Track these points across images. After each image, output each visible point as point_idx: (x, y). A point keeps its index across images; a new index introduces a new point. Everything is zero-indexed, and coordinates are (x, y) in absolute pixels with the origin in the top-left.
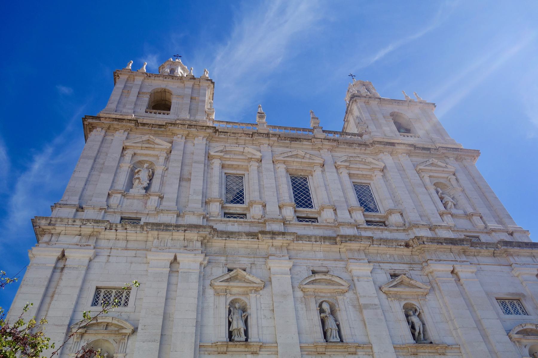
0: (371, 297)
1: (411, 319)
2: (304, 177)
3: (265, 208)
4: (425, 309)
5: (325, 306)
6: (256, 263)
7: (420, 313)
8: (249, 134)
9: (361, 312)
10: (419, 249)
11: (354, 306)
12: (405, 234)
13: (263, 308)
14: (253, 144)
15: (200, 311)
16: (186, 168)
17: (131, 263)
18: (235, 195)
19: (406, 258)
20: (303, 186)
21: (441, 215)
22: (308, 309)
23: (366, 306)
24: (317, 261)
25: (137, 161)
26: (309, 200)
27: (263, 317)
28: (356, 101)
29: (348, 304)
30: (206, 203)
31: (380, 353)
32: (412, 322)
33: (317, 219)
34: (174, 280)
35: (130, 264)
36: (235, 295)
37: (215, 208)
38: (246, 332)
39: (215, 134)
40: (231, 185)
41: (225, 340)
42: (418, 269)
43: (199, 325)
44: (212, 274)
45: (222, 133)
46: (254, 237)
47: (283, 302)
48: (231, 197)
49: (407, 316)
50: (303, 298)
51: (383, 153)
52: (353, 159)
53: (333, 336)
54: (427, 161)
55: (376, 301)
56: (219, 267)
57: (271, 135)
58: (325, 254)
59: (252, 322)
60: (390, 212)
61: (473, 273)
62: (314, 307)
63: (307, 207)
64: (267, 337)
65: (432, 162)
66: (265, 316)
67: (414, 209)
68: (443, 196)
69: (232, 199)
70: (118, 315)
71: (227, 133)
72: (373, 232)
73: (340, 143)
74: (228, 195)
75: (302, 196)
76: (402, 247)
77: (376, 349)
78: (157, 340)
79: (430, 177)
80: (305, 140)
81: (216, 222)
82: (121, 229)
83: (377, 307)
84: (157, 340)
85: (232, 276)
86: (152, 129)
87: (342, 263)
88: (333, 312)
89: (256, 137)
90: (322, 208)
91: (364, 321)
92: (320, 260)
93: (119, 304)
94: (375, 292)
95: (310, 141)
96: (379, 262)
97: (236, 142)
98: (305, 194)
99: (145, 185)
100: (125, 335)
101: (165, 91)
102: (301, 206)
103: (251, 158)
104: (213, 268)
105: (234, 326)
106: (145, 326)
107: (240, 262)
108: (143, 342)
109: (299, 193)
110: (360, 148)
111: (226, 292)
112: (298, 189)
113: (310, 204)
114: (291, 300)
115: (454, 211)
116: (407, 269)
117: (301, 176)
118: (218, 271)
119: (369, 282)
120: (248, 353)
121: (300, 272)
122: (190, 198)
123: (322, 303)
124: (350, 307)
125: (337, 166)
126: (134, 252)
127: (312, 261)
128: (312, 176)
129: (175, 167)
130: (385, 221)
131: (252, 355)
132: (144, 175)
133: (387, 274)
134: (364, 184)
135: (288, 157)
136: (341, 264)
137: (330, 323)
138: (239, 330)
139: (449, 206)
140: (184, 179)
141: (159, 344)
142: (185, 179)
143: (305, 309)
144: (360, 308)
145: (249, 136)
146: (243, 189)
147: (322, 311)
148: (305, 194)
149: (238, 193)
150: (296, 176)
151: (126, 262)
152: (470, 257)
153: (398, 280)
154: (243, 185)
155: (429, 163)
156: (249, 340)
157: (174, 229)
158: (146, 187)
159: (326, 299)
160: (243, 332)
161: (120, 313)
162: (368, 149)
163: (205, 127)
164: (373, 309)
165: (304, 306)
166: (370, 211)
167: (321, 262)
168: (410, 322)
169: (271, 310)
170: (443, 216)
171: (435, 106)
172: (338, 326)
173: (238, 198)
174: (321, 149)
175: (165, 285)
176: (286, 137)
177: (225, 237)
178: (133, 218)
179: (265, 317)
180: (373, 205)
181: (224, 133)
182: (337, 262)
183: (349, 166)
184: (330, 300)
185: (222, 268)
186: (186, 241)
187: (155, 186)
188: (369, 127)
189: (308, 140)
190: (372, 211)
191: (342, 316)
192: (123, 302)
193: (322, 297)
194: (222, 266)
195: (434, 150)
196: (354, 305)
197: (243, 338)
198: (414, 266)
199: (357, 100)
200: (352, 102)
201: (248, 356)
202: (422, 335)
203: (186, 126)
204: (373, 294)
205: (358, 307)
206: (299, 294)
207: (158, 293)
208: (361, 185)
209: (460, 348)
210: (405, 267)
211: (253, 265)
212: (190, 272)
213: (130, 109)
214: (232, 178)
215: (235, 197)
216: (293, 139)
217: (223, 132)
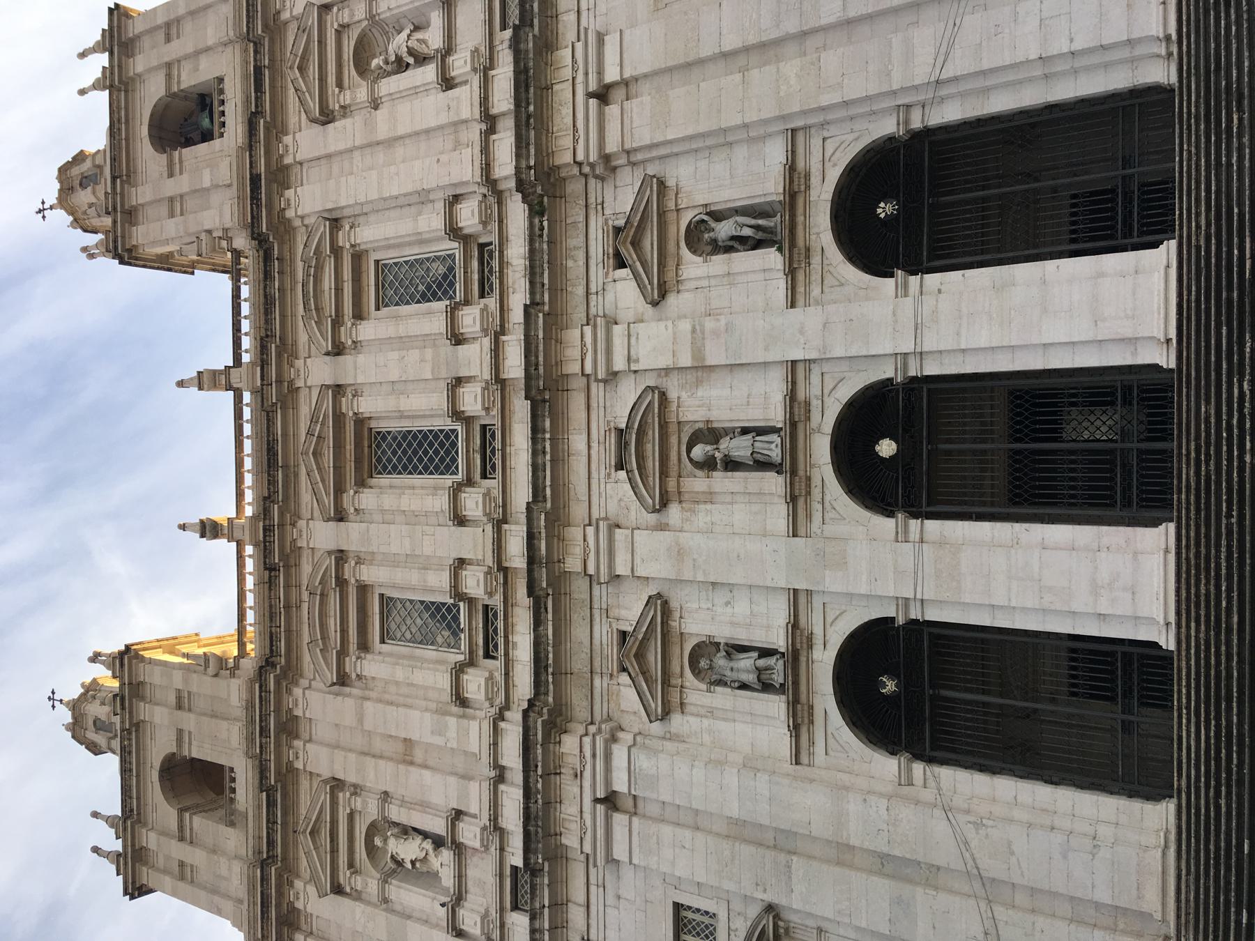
0: (674, 338)
1: (723, 241)
2: (376, 438)
3: (467, 561)
4: (701, 199)
5: (699, 451)
6: (604, 606)
7: (707, 214)
8: (270, 577)
9: (712, 368)
10: (549, 179)
11: (698, 383)
12: (508, 200)
13: (710, 605)
14: (296, 565)
16: (378, 745)
17: (619, 897)
18: (438, 625)
19: (573, 216)
20: (400, 445)
21: (447, 83)
22: (710, 497)
23: (698, 352)
24: (594, 452)
25: (366, 858)
26: (436, 436)
27: (729, 610)
28: (129, 251)
29: (694, 396)
31: (806, 346)
32: (733, 238)
33: (484, 427)
35: (621, 900)
36: (682, 667)
38: (765, 653)
39: (278, 666)
40: (412, 630)
41: (783, 706)
42: (599, 192)
44: (635, 713)
45: (274, 648)
46: (542, 605)
47: (694, 560)
48: (443, 633)
49: (718, 248)
50: (684, 505)
51: (284, 209)
52: (312, 299)
53: (773, 448)
54: (295, 88)
55: (685, 326)
56: (617, 695)
57: (267, 522)
58: (574, 429)
59: (743, 636)
60: (453, 231)
61: (603, 40)
63: (454, 444)
65: (297, 71)
66: (727, 603)
67: (438, 160)
68: (393, 58)
69: (446, 633)
70: (735, 935)
71: (271, 634)
72: (511, 290)
73: (269, 333)
74: (440, 640)
75: (426, 452)
76: (545, 224)
77: (797, 355)
78: (788, 862)
79: (340, 84)
80: (271, 429)
81: (511, 687)
82: (542, 920)
83: (698, 327)
84: (788, 862)
85: (638, 670)
86: (279, 822)
87: (594, 386)
89: (277, 561)
90: (456, 414)
91: (732, 367)
92: (589, 447)
93: (711, 928)
94: (662, 325)
95: (271, 414)
96: (588, 293)
97: (294, 609)
98: (420, 445)
99: (428, 845)
100: (776, 927)
101: (169, 769)
102: (454, 460)
103: (337, 578)
104: (622, 707)
105: (750, 678)
106: (757, 885)
107: (604, 641)
108: (792, 891)
109: (420, 460)
110: (276, 275)
112: (410, 460)
113: (447, 436)
114: (684, 538)
115: (434, 38)
116: (601, 220)
117: (374, 446)
119: (638, 334)
120: (810, 656)
121: (620, 500)
122: (455, 746)
123: (691, 460)
124: (700, 393)
125: (335, 350)
126: (593, 889)
127: (594, 466)
128: (370, 418)
130: (478, 244)
131: (814, 647)
133: (616, 277)
134: (380, 279)
135: (323, 481)
137: (740, 448)
138: (759, 671)
139: (423, 49)
140: (408, 753)
141: (795, 858)
142: (406, 750)
143: (709, 506)
144: (702, 370)
145: (276, 576)
146: (422, 602)
147: (708, 465)
148: (420, 445)
149: (433, 616)
150: (374, 460)
151: (618, 909)
152: (560, 32)
153: (628, 253)
154: (411, 601)
155: (300, 79)
156: (782, 650)
157: (536, 802)
158: (433, 845)
159: (684, 448)
160: (762, 663)
161: (731, 932)
162: (276, 252)
163: (263, 694)
164: (703, 339)
165: (702, 507)
166: (454, 276)
167: (594, 445)
168: (731, 243)
169: (713, 589)
170: (453, 78)
171: (117, 5)
172: (745, 431)
173: (444, 618)
174: (291, 382)
175: (667, 831)
176: (269, 480)
177: (547, 675)
178: (514, 883)
179: (730, 603)
180: (435, 265)
181: (274, 643)
182: (594, 404)
183: (334, 317)
184: (685, 440)
185: (622, 688)
186: (563, 771)
188: (206, 227)
189: (268, 420)
190: (451, 269)
191: (723, 416)
192: (706, 920)
193: (679, 460)
194: (615, 687)
195: (258, 56)
196: (695, 380)
198: (592, 200)
199: (127, 247)
200: (136, 260)
201: (815, 657)
202: (760, 222)
203: (264, 740)
204: (667, 329)
205: (700, 374)
206: (674, 511)
207: (684, 847)
208: (383, 286)
209: (792, 130)
211: (611, 614)
212: (635, 770)
213: (230, 869)
214: (393, 626)
215: (442, 625)
216: (272, 461)
217: (271, 645)
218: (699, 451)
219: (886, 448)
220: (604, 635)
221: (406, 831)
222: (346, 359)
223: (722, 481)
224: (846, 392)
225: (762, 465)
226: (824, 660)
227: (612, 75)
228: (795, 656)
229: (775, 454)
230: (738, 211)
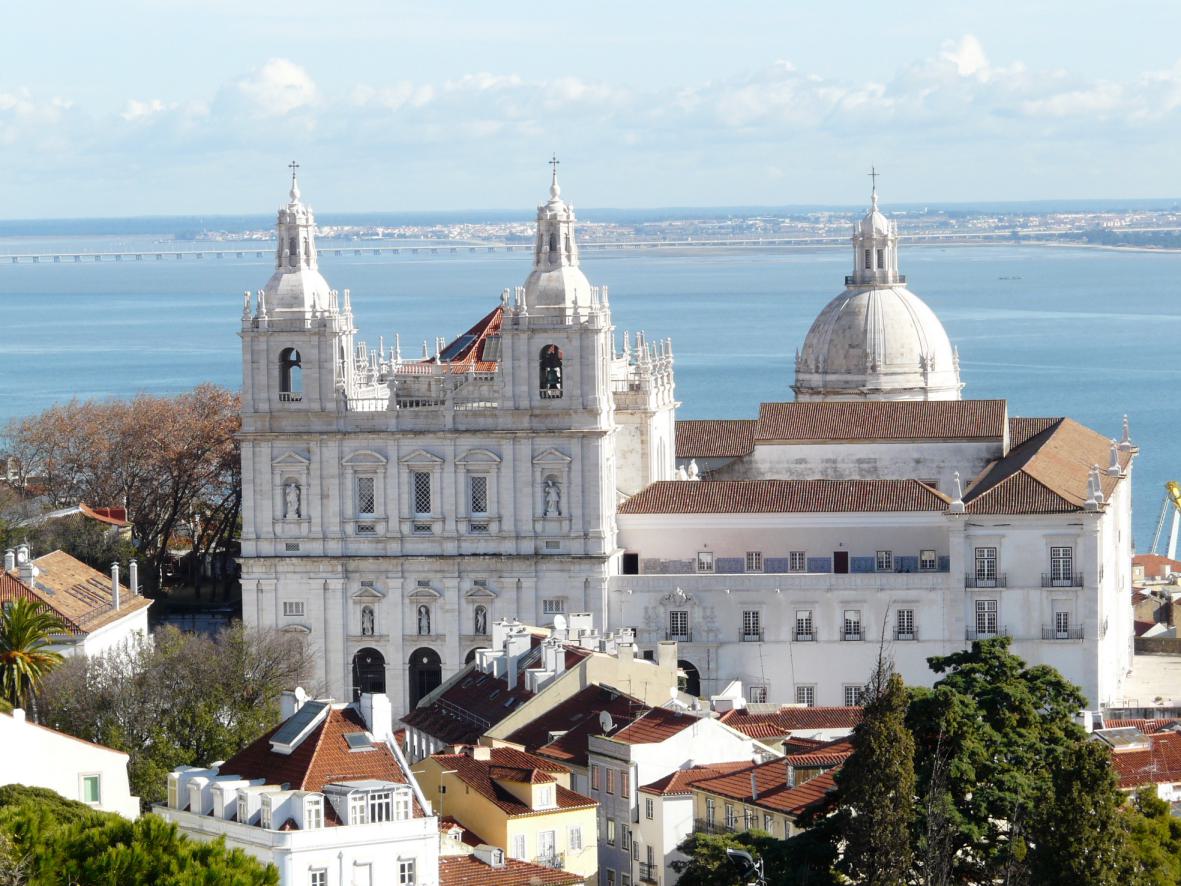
5: (423, 610)
15: (345, 616)
30: (343, 522)
34: (327, 595)
37: (350, 528)
38: (372, 629)
43: (345, 626)
49: (477, 614)
64: (384, 632)
88: (427, 612)
111: (360, 602)
118: (355, 587)
129: (316, 490)
137: (424, 623)
147: (420, 612)
187: (304, 512)
191: (432, 616)
197: (370, 633)
219: (425, 660)
220: (370, 577)
223: (415, 617)
224: (438, 651)
225: (420, 628)
226: (373, 645)
229: (422, 633)
230: (485, 623)
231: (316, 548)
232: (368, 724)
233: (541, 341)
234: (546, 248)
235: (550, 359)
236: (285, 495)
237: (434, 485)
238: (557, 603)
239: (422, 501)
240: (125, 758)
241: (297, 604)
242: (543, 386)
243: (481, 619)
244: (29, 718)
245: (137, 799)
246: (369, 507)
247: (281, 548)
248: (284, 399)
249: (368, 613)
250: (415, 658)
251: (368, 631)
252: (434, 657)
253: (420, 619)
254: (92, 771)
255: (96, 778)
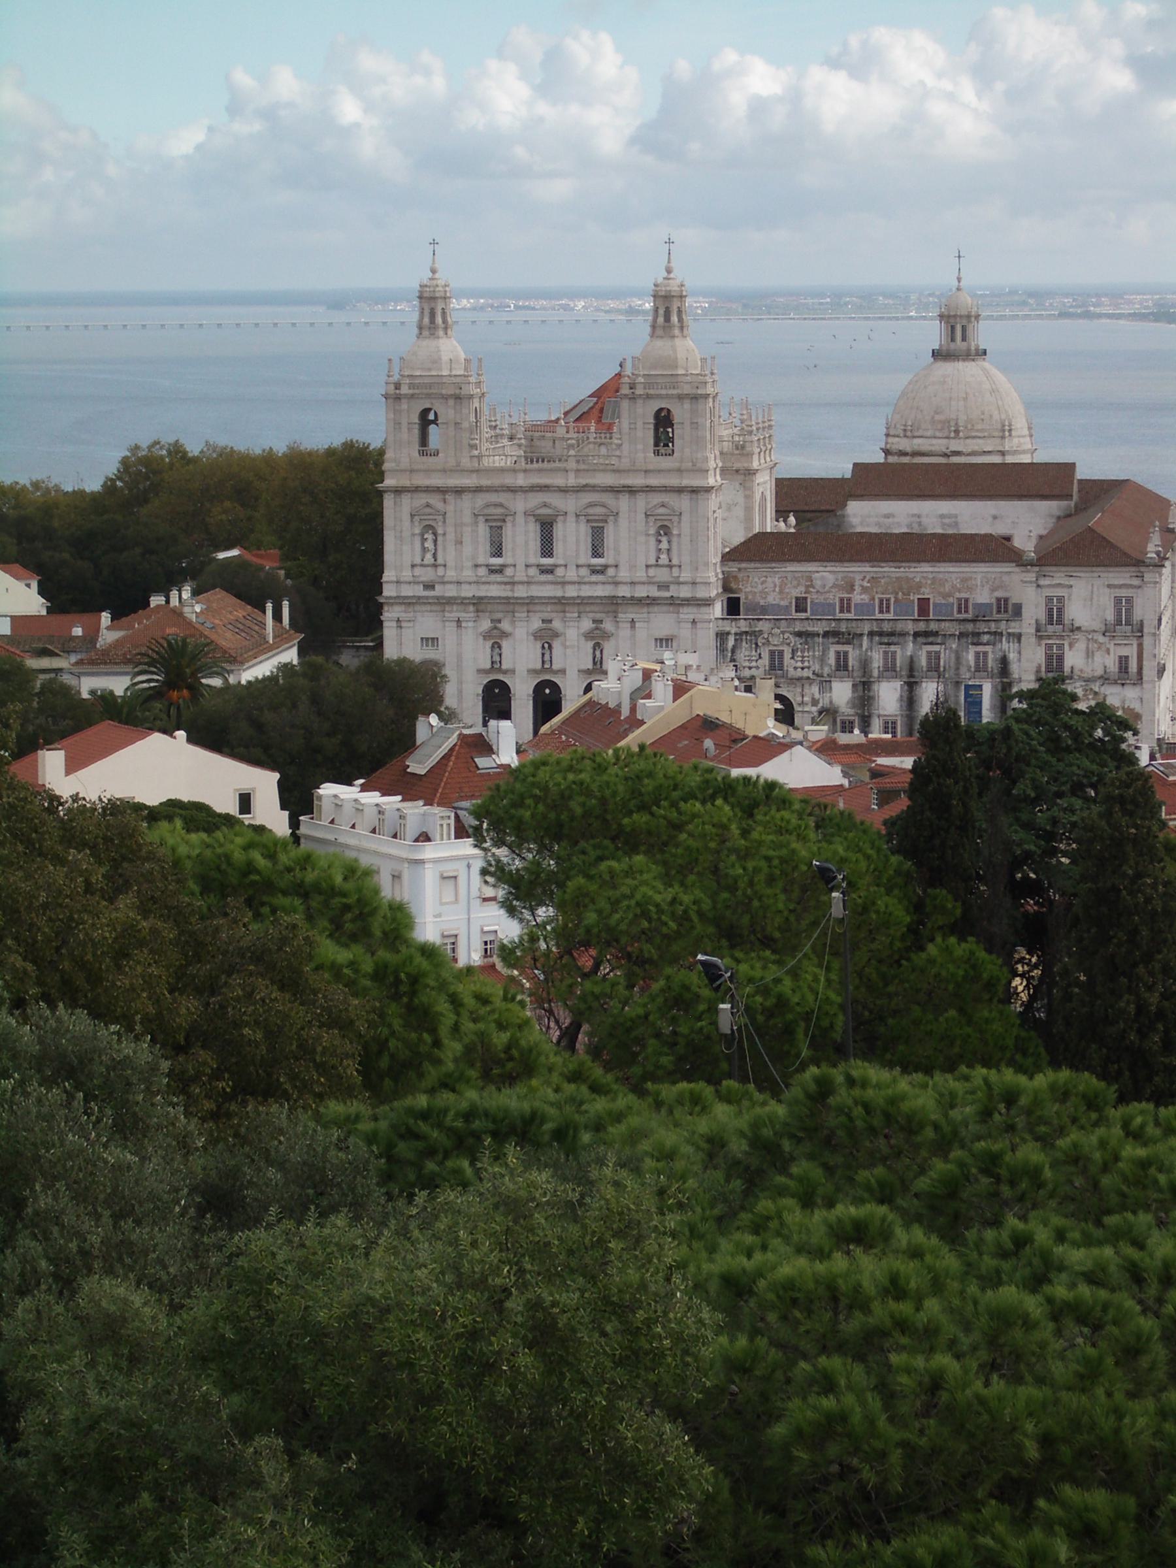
5: (546, 645)
49: (594, 650)
53: (547, 666)
62: (539, 645)
88: (550, 647)
129: (451, 536)
132: (429, 544)
136: (562, 614)
137: (547, 657)
147: (543, 647)
191: (554, 651)
210: (603, 615)
218: (546, 645)
219: (547, 691)
220: (499, 616)
221: (435, 541)
222: (574, 519)
223: (539, 651)
225: (543, 662)
226: (501, 677)
227: (637, 625)
228: (500, 670)
231: (451, 591)
232: (494, 747)
233: (656, 405)
234: (661, 320)
235: (663, 421)
236: (424, 540)
237: (559, 530)
238: (667, 640)
239: (547, 548)
240: (277, 776)
241: (433, 639)
242: (656, 444)
243: (598, 653)
244: (190, 740)
245: (287, 813)
246: (498, 553)
247: (419, 591)
248: (422, 453)
249: (497, 646)
250: (539, 688)
251: (495, 666)
252: (555, 688)
253: (543, 655)
254: (245, 787)
255: (249, 794)
